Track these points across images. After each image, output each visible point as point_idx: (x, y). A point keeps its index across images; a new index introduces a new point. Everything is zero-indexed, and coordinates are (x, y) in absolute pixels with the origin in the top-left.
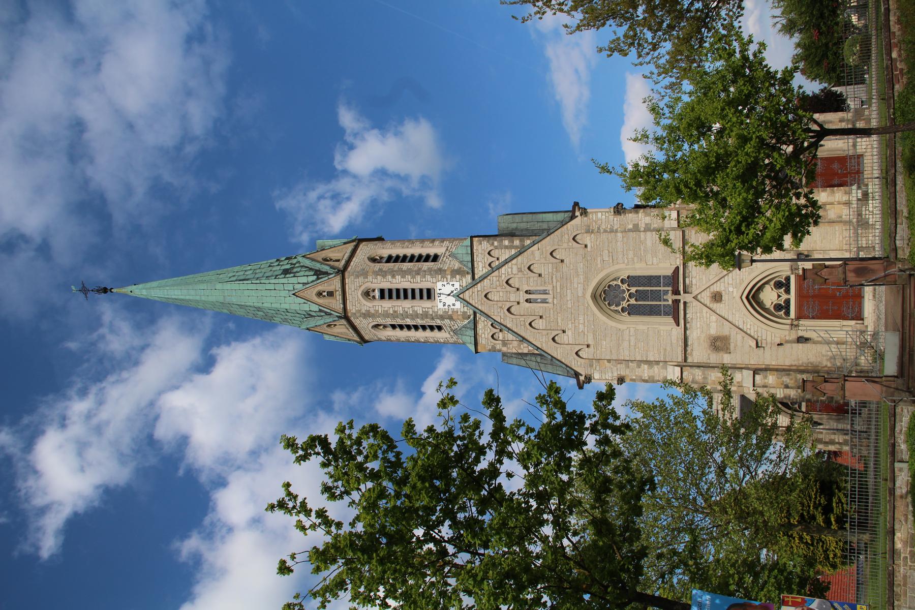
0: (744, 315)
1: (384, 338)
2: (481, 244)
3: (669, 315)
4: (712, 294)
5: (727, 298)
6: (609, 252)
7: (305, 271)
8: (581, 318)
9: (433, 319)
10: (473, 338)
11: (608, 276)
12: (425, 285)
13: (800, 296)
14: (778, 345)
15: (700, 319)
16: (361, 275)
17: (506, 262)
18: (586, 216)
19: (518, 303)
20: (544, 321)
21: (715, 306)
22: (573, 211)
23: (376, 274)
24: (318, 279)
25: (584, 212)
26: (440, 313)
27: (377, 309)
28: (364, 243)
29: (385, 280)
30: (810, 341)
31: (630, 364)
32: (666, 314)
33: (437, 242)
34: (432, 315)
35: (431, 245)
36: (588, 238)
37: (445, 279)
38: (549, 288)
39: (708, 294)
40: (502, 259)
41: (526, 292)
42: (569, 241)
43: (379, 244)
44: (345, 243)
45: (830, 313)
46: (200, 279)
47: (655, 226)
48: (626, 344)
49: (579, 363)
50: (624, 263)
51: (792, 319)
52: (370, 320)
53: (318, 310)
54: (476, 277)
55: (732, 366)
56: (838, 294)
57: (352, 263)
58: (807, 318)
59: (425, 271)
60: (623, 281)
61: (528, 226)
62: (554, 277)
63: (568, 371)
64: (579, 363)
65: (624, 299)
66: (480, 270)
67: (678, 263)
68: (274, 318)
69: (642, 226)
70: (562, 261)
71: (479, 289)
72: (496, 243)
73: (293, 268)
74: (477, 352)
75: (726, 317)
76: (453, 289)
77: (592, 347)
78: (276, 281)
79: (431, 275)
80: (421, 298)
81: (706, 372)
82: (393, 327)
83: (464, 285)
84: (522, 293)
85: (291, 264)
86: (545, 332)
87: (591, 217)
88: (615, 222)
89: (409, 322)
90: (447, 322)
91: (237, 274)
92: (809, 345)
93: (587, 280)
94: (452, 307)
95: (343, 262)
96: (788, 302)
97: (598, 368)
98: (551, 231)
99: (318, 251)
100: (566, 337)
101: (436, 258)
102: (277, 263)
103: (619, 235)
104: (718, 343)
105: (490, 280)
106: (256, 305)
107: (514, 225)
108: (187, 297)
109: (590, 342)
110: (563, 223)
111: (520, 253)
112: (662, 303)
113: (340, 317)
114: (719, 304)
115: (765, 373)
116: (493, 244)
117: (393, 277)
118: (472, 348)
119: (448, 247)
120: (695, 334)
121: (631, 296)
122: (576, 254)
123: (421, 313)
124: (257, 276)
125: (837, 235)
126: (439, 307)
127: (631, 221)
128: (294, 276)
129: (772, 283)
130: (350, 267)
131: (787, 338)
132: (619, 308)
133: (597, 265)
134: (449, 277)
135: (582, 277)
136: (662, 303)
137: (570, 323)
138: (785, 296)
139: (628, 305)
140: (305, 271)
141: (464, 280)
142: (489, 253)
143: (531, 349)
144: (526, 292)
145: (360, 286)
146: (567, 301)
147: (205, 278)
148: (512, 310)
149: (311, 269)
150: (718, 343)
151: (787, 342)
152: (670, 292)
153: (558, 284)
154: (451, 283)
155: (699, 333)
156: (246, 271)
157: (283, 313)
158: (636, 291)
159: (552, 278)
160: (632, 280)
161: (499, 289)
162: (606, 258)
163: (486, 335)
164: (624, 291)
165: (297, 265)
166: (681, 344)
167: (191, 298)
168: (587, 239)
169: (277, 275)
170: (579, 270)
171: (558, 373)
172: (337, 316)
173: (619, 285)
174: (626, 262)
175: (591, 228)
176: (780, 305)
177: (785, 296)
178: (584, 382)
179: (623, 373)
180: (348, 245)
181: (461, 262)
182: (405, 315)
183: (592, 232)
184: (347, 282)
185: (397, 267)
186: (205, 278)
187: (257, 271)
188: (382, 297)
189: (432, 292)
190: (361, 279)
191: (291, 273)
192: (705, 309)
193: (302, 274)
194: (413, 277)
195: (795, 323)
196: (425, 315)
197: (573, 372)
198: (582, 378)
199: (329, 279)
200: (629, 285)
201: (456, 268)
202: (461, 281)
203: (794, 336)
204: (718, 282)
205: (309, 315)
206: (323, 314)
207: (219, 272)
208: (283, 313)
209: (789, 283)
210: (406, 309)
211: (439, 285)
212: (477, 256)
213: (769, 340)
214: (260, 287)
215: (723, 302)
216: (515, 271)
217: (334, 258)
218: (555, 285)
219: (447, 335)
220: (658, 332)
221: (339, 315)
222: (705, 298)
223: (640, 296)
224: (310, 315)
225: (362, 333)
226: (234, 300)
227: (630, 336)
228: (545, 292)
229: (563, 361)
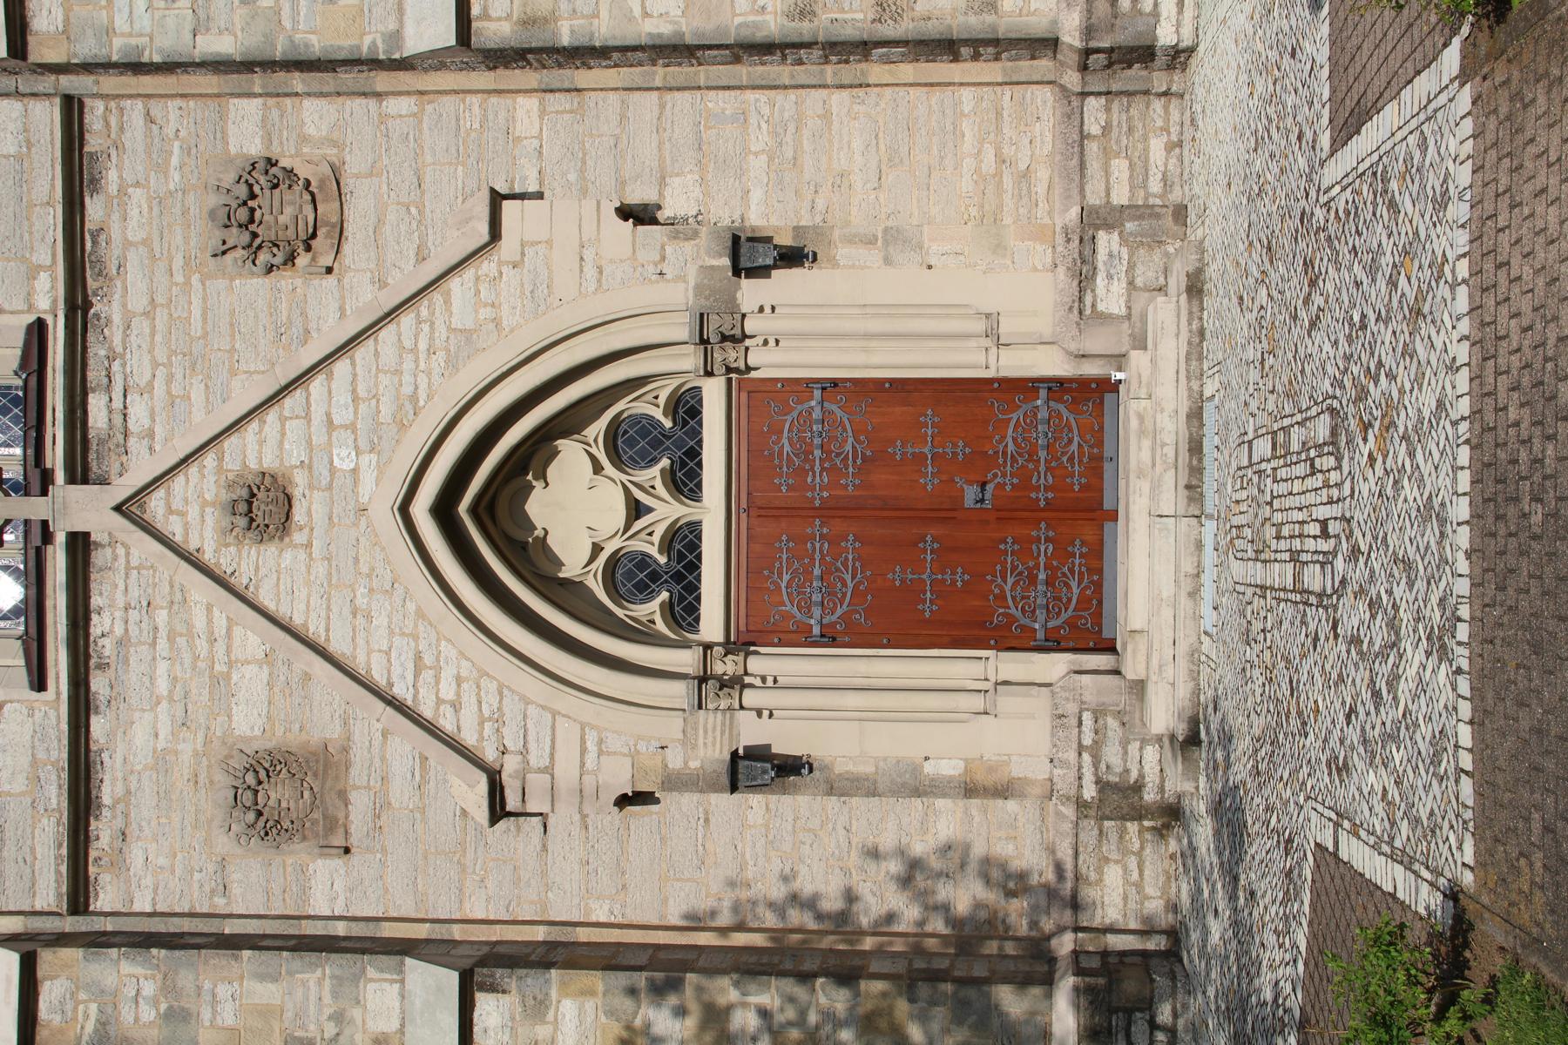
0: (420, 614)
4: (230, 486)
5: (319, 511)
14: (623, 801)
15: (171, 639)
30: (806, 778)
45: (927, 609)
51: (708, 647)
55: (358, 930)
56: (970, 494)
58: (800, 637)
67: (43, 304)
75: (315, 630)
81: (185, 979)
92: (802, 800)
96: (685, 541)
104: (278, 794)
114: (271, 550)
115: (531, 980)
120: (140, 735)
125: (969, 143)
129: (597, 429)
131: (675, 760)
138: (667, 510)
150: (278, 794)
151: (677, 782)
166: (55, 794)
176: (643, 560)
177: (667, 510)
192: (201, 589)
195: (726, 666)
203: (712, 752)
204: (272, 416)
213: (567, 770)
215: (298, 537)
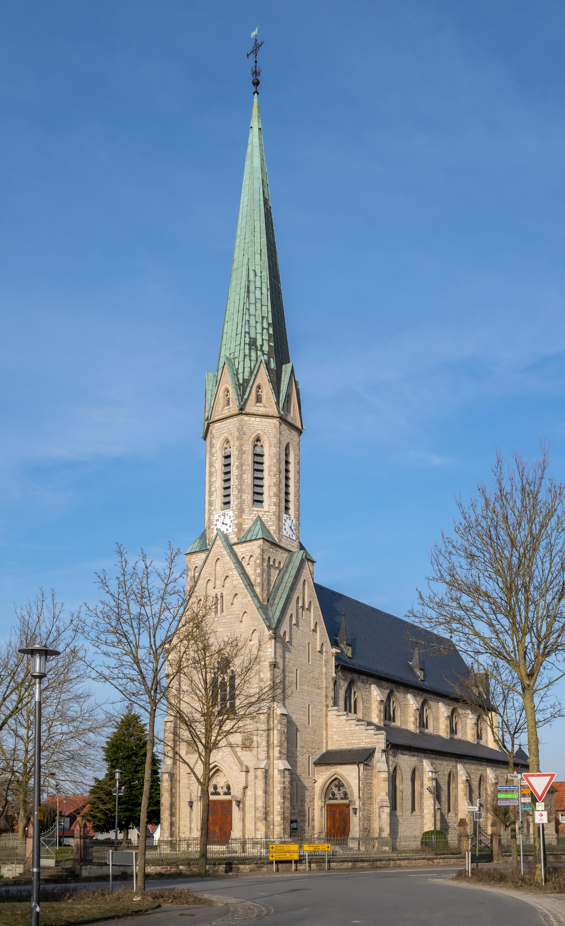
2: (259, 547)
7: (250, 368)
24: (239, 385)
33: (275, 500)
35: (272, 494)
37: (234, 518)
38: (224, 613)
54: (235, 547)
57: (253, 419)
59: (241, 498)
62: (232, 616)
73: (257, 350)
85: (262, 346)
96: (218, 794)
101: (258, 502)
119: (268, 512)
128: (245, 356)
140: (250, 368)
153: (227, 620)
154: (231, 524)
156: (261, 288)
159: (231, 615)
181: (249, 531)
191: (250, 350)
203: (194, 798)
210: (214, 484)
212: (250, 546)
216: (235, 582)
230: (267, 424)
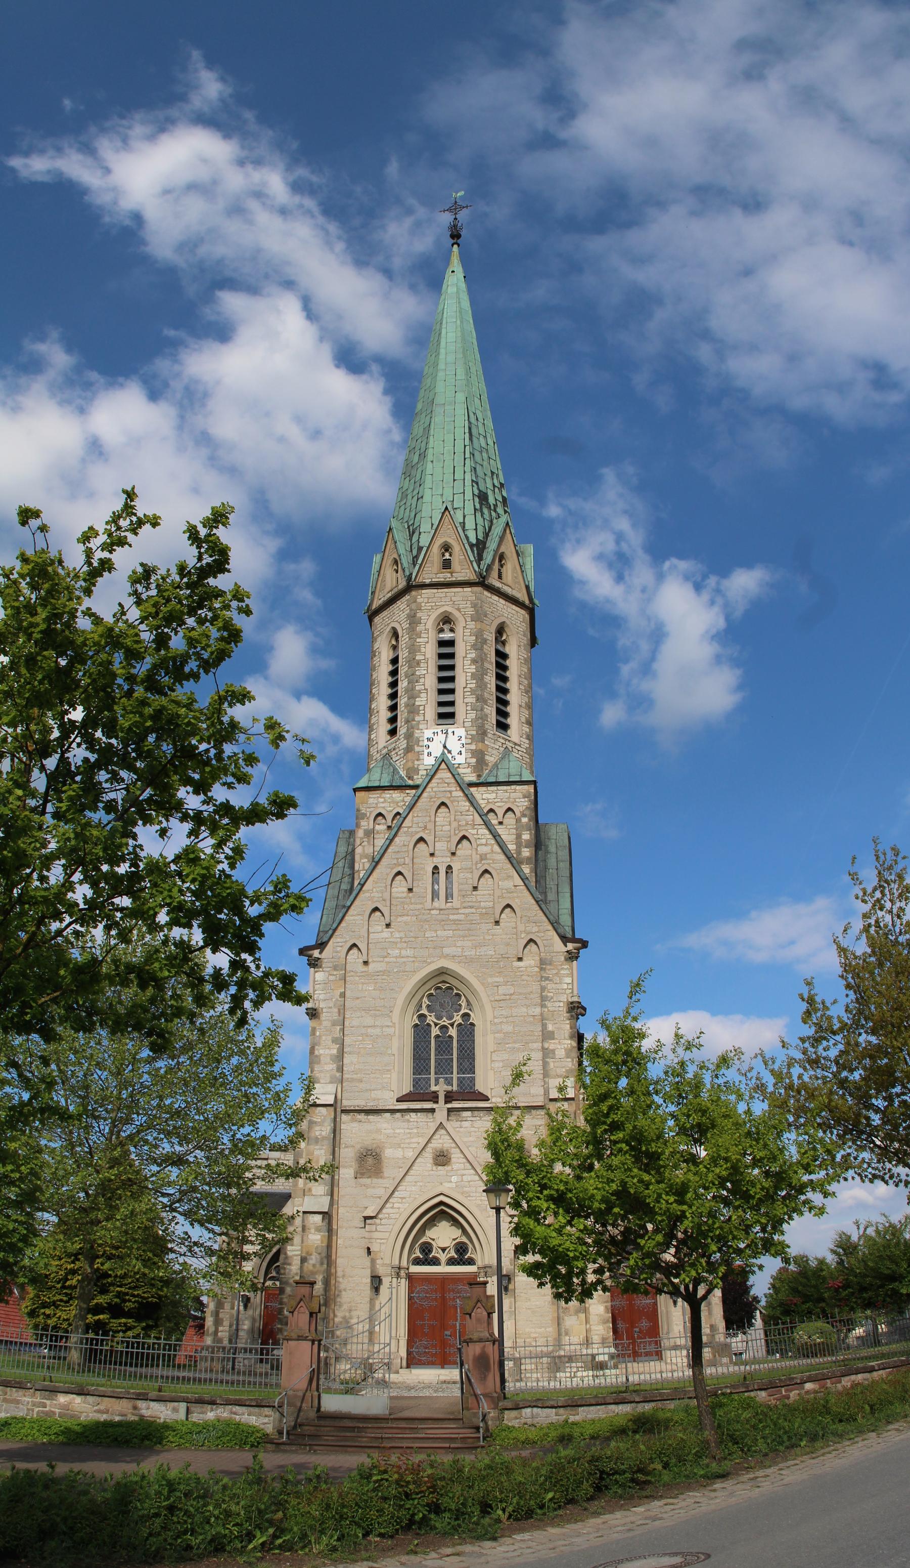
1: (376, 646)
2: (524, 797)
3: (414, 1086)
4: (447, 1151)
6: (511, 995)
8: (409, 952)
9: (407, 722)
10: (377, 784)
11: (474, 992)
12: (460, 709)
13: (444, 1281)
14: (369, 1249)
16: (477, 612)
17: (496, 836)
18: (566, 960)
19: (432, 855)
20: (405, 895)
21: (428, 1155)
22: (574, 940)
23: (479, 635)
24: (471, 546)
25: (572, 957)
26: (417, 733)
27: (423, 635)
28: (527, 617)
29: (469, 648)
30: (374, 1294)
31: (338, 1028)
32: (416, 1083)
33: (528, 730)
34: (414, 720)
35: (523, 720)
36: (532, 963)
37: (470, 741)
38: (456, 902)
39: (446, 1146)
40: (500, 830)
41: (449, 867)
42: (528, 933)
43: (526, 640)
44: (527, 587)
45: (418, 1323)
46: (473, 370)
47: (552, 1065)
48: (369, 1021)
49: (339, 949)
50: (495, 1017)
51: (408, 1269)
52: (406, 625)
53: (421, 544)
54: (473, 790)
55: (336, 1182)
57: (496, 598)
58: (411, 1290)
59: (482, 710)
60: (466, 1016)
61: (552, 871)
62: (473, 910)
63: (327, 932)
64: (339, 949)
65: (439, 1017)
66: (483, 796)
67: (494, 1100)
68: (408, 479)
69: (551, 1045)
70: (497, 923)
71: (454, 794)
72: (525, 820)
73: (489, 508)
74: (355, 790)
75: (411, 1172)
76: (454, 753)
77: (365, 969)
78: (468, 482)
79: (477, 718)
80: (441, 704)
81: (326, 1142)
82: (395, 661)
83: (461, 771)
84: (448, 860)
85: (496, 506)
86: (387, 895)
87: (566, 967)
88: (557, 1004)
89: (403, 685)
90: (403, 744)
91: (480, 425)
92: (369, 1292)
93: (468, 961)
94: (426, 752)
95: (497, 584)
96: (435, 1262)
97: (331, 978)
98: (543, 906)
99: (515, 546)
100: (379, 928)
101: (503, 726)
102: (497, 484)
103: (538, 1010)
104: (370, 1160)
105: (468, 811)
106: (430, 452)
107: (552, 849)
108: (442, 351)
109: (372, 966)
110: (555, 924)
111: (509, 858)
112: (433, 1076)
113: (409, 578)
114: (431, 1161)
115: (325, 1228)
116: (524, 815)
117: (474, 661)
118: (362, 783)
119: (519, 746)
120: (385, 1125)
121: (444, 1028)
122: (508, 944)
123: (417, 703)
124: (477, 454)
125: (538, 1330)
126: (425, 731)
127: (558, 1028)
128: (475, 510)
129: (464, 1239)
130: (489, 595)
131: (379, 1262)
132: (424, 1011)
133: (491, 976)
134: (473, 747)
135: (473, 953)
136: (433, 1076)
137: (402, 934)
138: (443, 1257)
139: (429, 1025)
140: (484, 527)
141: (469, 770)
142: (509, 809)
143: (361, 875)
144: (449, 867)
145: (459, 610)
146: (436, 931)
147: (474, 377)
148: (422, 845)
149: (487, 535)
150: (370, 1160)
151: (373, 1262)
152: (449, 1088)
153: (462, 917)
155: (388, 1131)
156: (485, 437)
157: (415, 492)
158: (451, 1037)
159: (471, 907)
160: (467, 1030)
161: (454, 824)
162: (502, 990)
163: (382, 805)
164: (450, 1018)
165: (493, 514)
166: (370, 1105)
167: (442, 356)
168: (530, 961)
169: (477, 483)
170: (485, 948)
171: (324, 917)
172: (411, 574)
173: (460, 1010)
174: (496, 1020)
175: (548, 967)
176: (430, 1251)
177: (443, 1257)
178: (310, 956)
179: (324, 1016)
180: (525, 591)
181: (496, 765)
182: (413, 679)
183: (541, 969)
184: (465, 589)
185: (490, 667)
186: (474, 377)
187: (485, 455)
188: (442, 643)
189: (450, 721)
190: (470, 611)
191: (481, 504)
192: (423, 1141)
193: (480, 520)
194: (473, 692)
195: (402, 1273)
196: (413, 710)
197: (325, 939)
198: (316, 953)
199: (471, 562)
200: (460, 1025)
201: (487, 757)
202: (466, 765)
203: (381, 1271)
204: (465, 1160)
205: (413, 531)
206: (415, 552)
207: (485, 397)
208: (415, 492)
209: (464, 1264)
210: (422, 680)
211: (461, 732)
212: (506, 791)
213: (376, 1235)
214: (459, 458)
215: (434, 1168)
216: (483, 850)
217: (503, 570)
218: (460, 911)
219: (382, 744)
220: (388, 1070)
221: (413, 577)
222: (441, 1141)
223: (444, 1043)
224: (414, 532)
225: (385, 613)
226: (437, 419)
227: (382, 1027)
228: (449, 896)
229: (343, 924)
230: (513, 612)
